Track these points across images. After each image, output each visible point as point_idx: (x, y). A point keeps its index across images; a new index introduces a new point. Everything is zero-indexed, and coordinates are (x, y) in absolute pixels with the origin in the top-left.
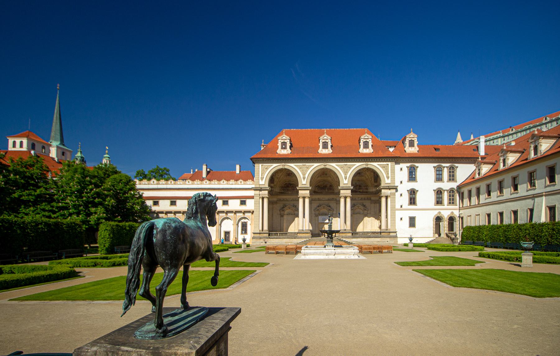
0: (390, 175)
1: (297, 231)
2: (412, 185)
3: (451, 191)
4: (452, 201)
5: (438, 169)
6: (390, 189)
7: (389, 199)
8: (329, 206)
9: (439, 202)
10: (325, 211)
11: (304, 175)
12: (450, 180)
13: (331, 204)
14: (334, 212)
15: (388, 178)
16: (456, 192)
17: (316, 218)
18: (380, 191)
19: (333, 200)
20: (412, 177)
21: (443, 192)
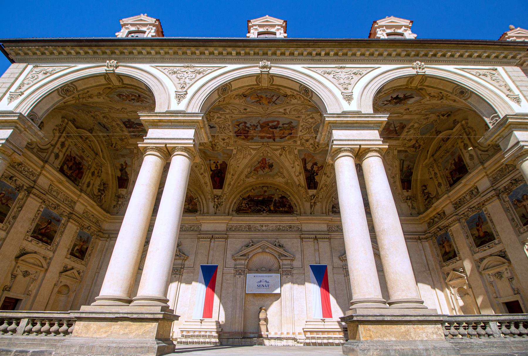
10: (267, 259)
13: (283, 241)
19: (291, 231)
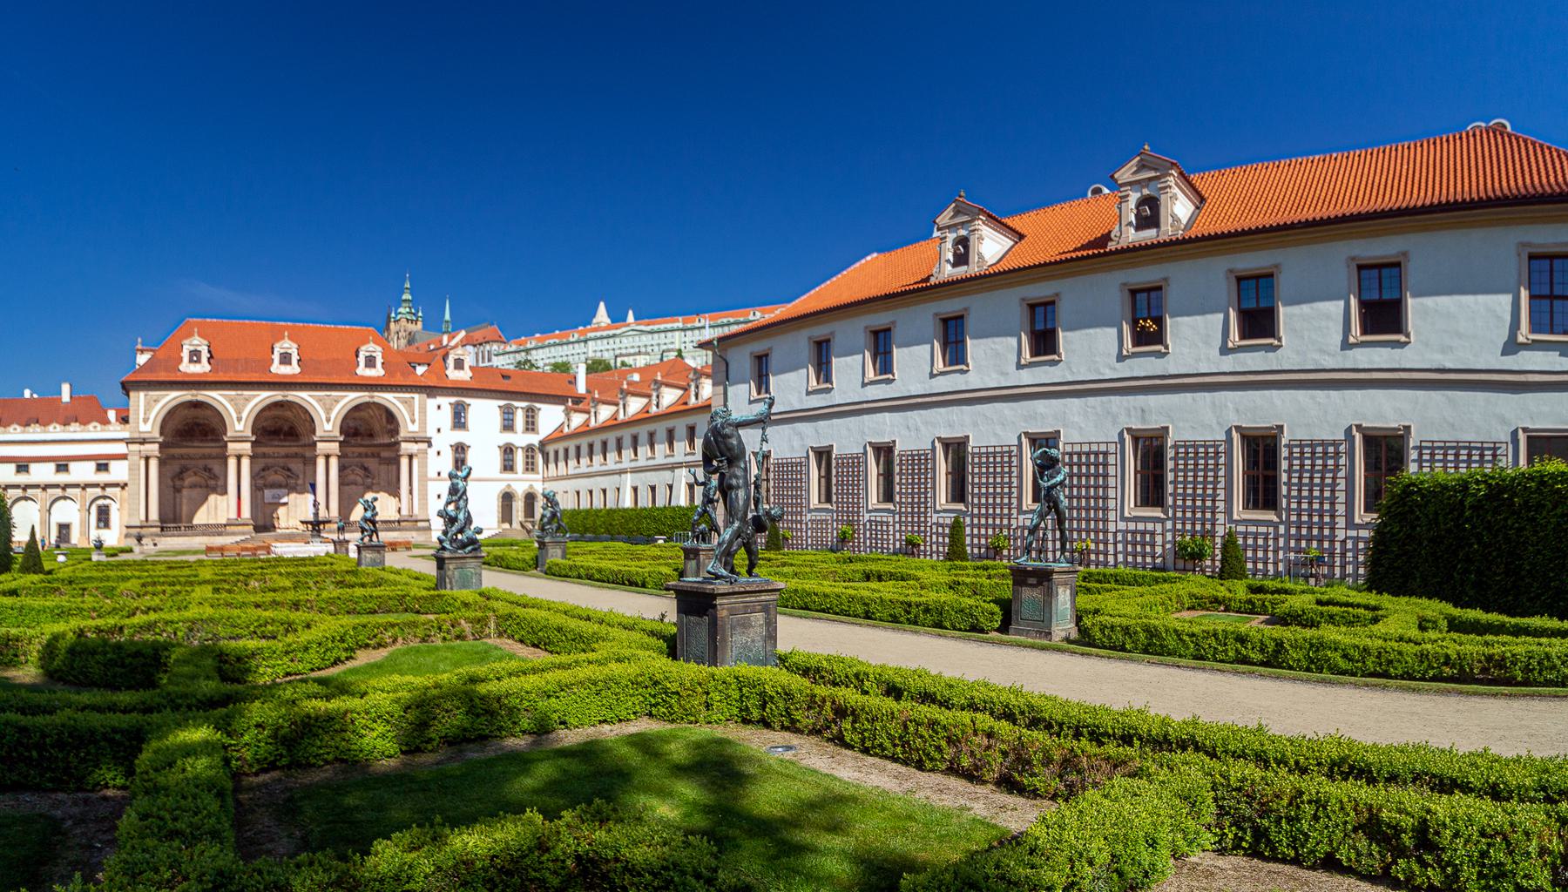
0: (417, 416)
1: (224, 522)
2: (459, 436)
3: (529, 449)
4: (530, 467)
6: (416, 442)
7: (415, 461)
8: (289, 470)
9: (508, 467)
10: (279, 478)
11: (239, 412)
12: (527, 429)
14: (300, 482)
15: (413, 421)
16: (537, 451)
17: (259, 494)
18: (397, 443)
20: (459, 422)
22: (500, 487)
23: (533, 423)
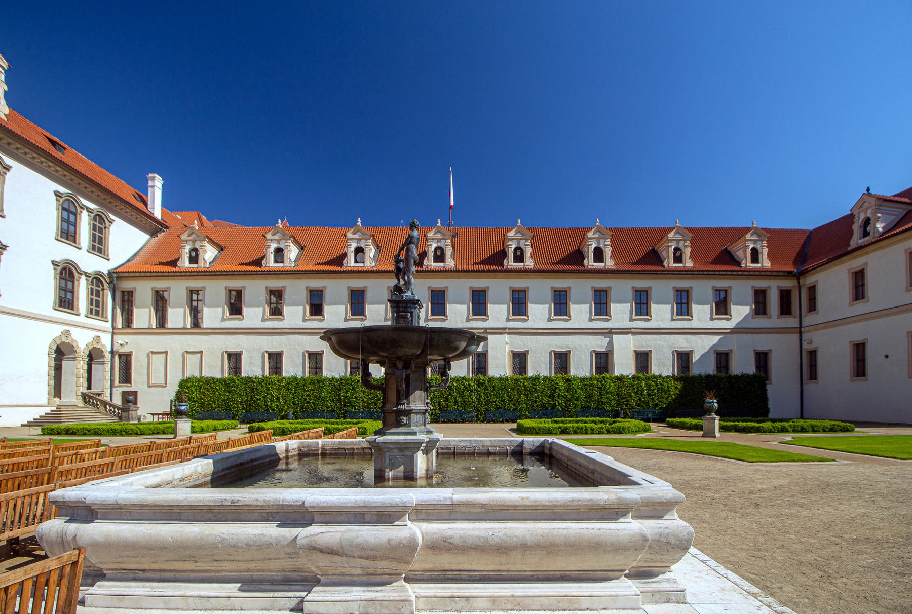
3: (96, 279)
5: (66, 206)
9: (66, 302)
12: (94, 248)
16: (106, 285)
21: (76, 275)
22: (56, 331)
23: (101, 241)
